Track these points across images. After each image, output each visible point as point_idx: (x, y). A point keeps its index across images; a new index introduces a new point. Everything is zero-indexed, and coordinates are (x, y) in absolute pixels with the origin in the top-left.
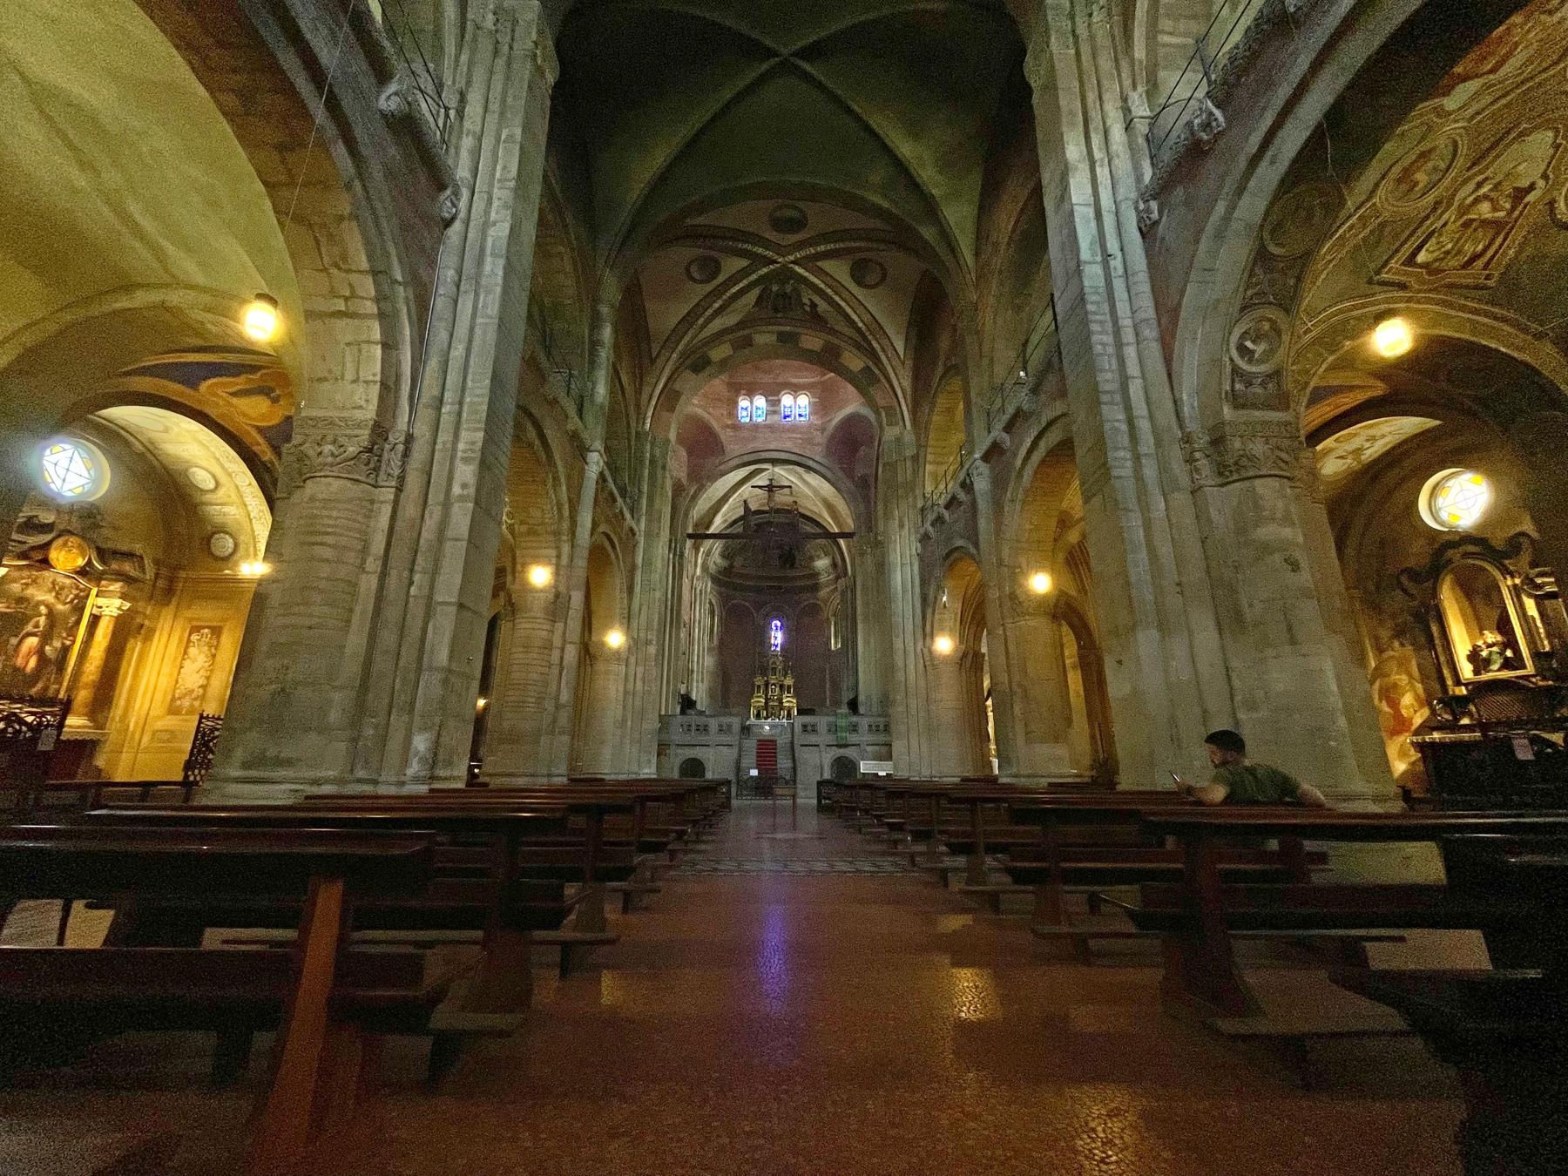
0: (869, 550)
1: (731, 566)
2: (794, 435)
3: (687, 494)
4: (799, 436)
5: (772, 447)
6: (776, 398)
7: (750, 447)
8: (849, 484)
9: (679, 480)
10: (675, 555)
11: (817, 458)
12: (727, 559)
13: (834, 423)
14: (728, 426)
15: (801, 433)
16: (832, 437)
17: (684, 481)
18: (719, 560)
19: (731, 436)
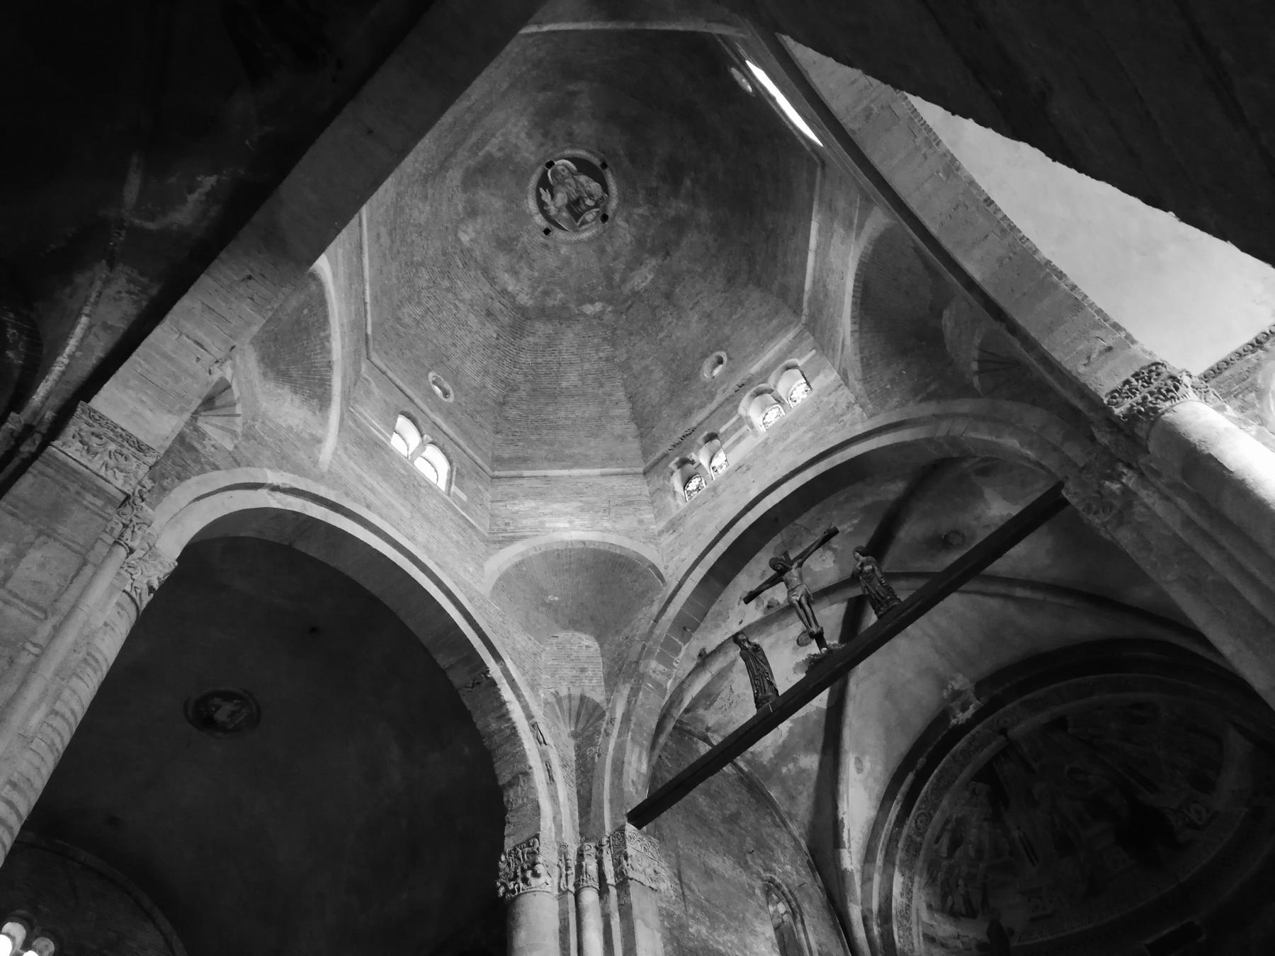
0: (1130, 479)
1: (998, 935)
2: (792, 437)
3: (612, 721)
4: (804, 428)
5: (754, 493)
6: (734, 419)
7: (711, 531)
8: (965, 406)
9: (583, 698)
10: (603, 891)
11: (860, 429)
12: (971, 914)
13: (849, 341)
14: (661, 533)
15: (802, 424)
16: (866, 365)
17: (598, 696)
18: (945, 928)
19: (669, 545)
